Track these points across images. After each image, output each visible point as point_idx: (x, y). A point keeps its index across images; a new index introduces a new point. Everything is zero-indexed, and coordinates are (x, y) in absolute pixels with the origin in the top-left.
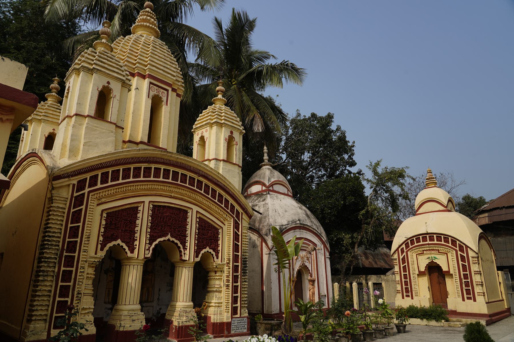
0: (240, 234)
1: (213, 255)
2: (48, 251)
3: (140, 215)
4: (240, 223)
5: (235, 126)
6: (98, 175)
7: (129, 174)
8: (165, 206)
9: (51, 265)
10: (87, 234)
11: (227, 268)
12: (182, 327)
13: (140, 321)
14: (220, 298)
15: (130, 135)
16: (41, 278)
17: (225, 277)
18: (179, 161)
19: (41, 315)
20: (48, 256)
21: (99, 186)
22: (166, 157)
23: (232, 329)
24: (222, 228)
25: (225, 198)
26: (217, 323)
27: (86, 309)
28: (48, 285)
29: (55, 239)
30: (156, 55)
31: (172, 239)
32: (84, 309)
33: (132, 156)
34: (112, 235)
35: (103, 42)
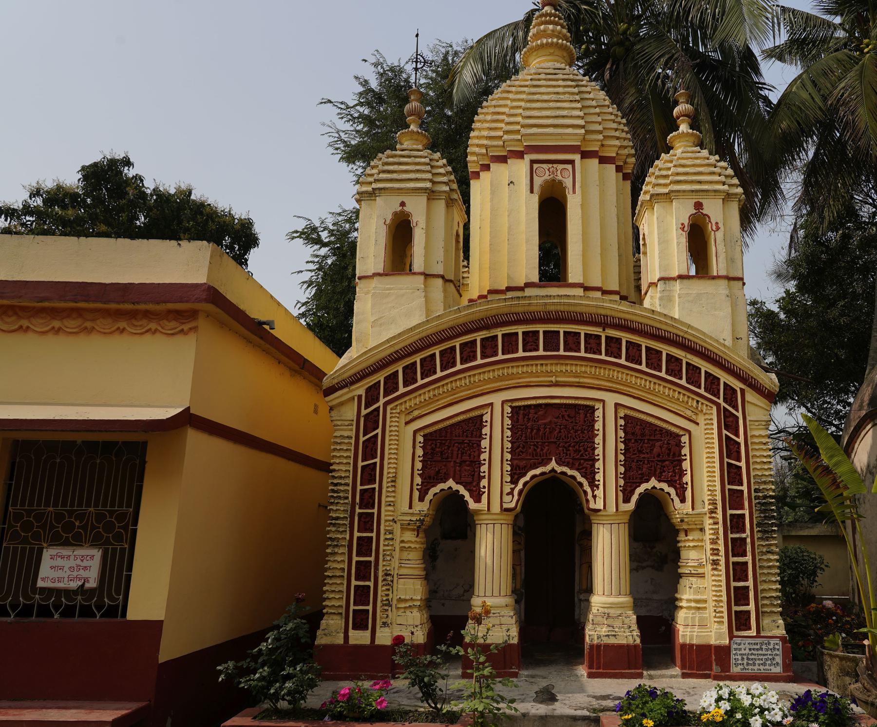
0: (741, 440)
1: (669, 494)
2: (334, 508)
3: (486, 430)
4: (740, 415)
5: (705, 187)
6: (397, 371)
7: (454, 358)
8: (540, 405)
9: (341, 529)
10: (391, 475)
11: (711, 521)
12: (598, 646)
13: (505, 628)
14: (698, 591)
15: (509, 277)
16: (329, 551)
17: (708, 542)
18: (552, 308)
19: (334, 606)
20: (334, 515)
21: (402, 390)
22: (520, 309)
23: (733, 661)
24: (689, 432)
25: (687, 363)
26: (691, 646)
27: (405, 601)
28: (339, 562)
29: (342, 488)
30: (538, 101)
31: (559, 469)
32: (400, 600)
33: (451, 324)
34: (438, 472)
35: (413, 132)
